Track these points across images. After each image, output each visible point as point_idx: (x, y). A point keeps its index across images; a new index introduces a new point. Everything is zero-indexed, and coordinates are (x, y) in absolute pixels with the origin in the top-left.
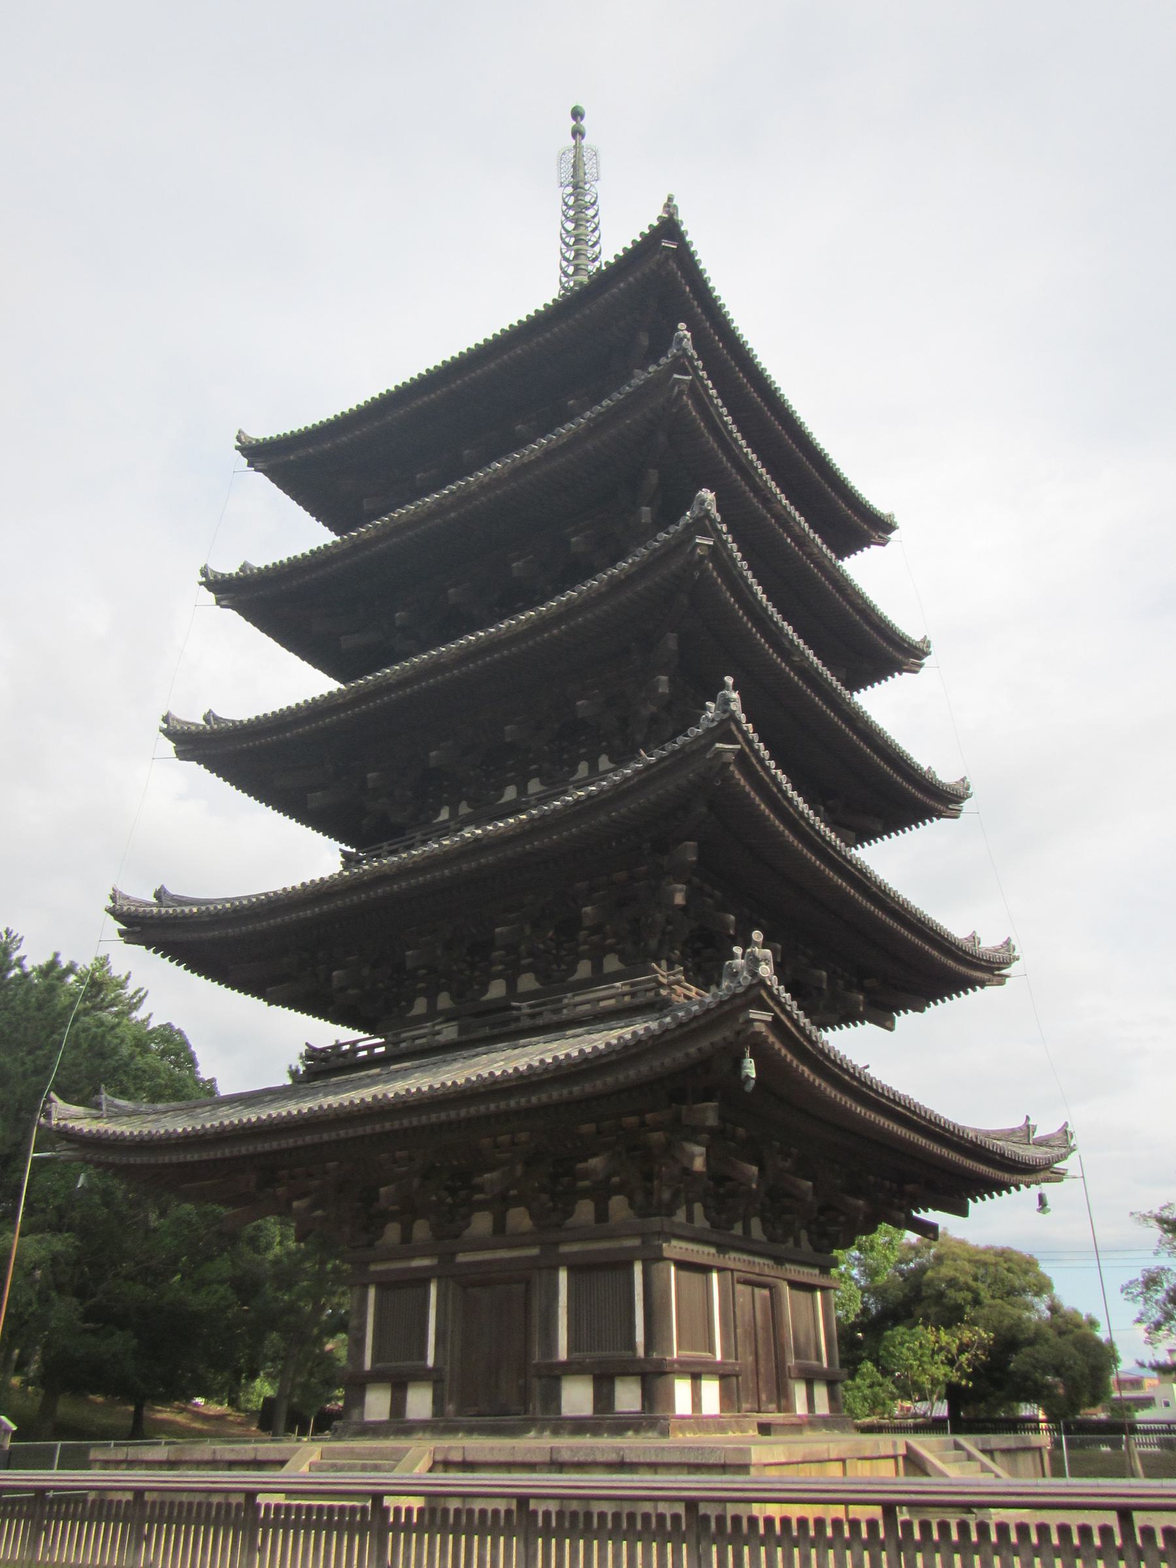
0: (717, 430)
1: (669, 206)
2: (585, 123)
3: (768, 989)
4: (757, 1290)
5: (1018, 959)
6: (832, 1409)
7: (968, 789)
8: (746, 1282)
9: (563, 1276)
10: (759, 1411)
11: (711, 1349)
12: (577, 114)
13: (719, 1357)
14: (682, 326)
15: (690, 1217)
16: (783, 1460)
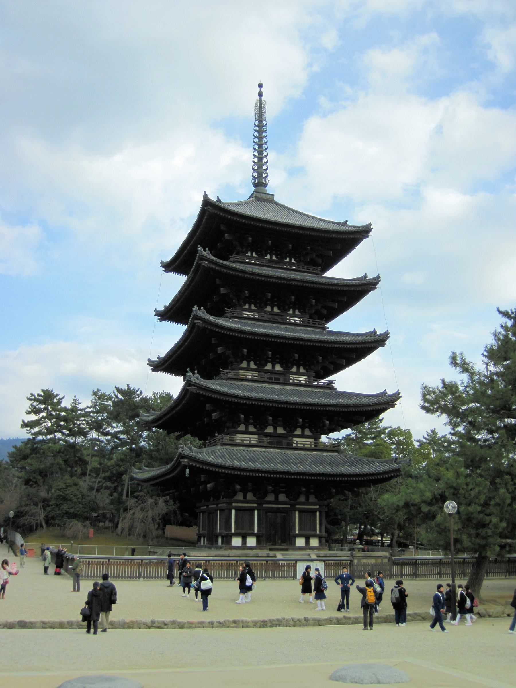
0: (225, 267)
1: (205, 196)
2: (262, 89)
3: (184, 454)
4: (279, 515)
5: (401, 397)
6: (320, 545)
7: (388, 334)
8: (270, 512)
9: (219, 512)
10: (276, 545)
11: (253, 530)
12: (260, 86)
13: (256, 531)
14: (199, 246)
15: (245, 497)
16: (205, 555)
